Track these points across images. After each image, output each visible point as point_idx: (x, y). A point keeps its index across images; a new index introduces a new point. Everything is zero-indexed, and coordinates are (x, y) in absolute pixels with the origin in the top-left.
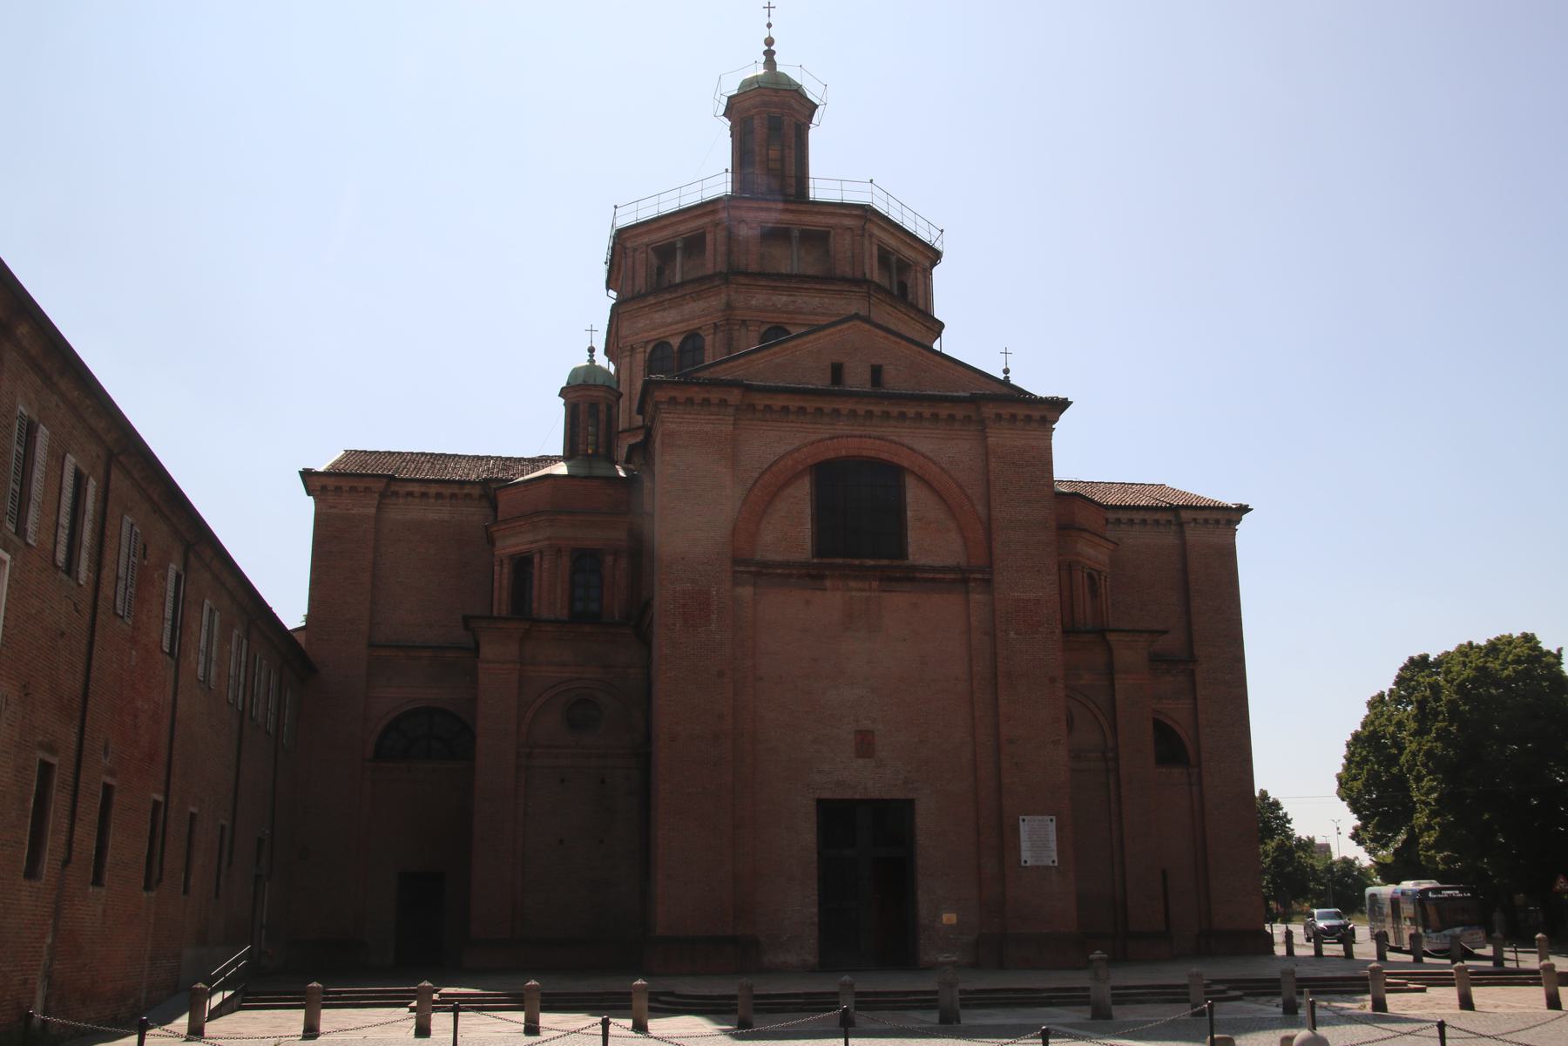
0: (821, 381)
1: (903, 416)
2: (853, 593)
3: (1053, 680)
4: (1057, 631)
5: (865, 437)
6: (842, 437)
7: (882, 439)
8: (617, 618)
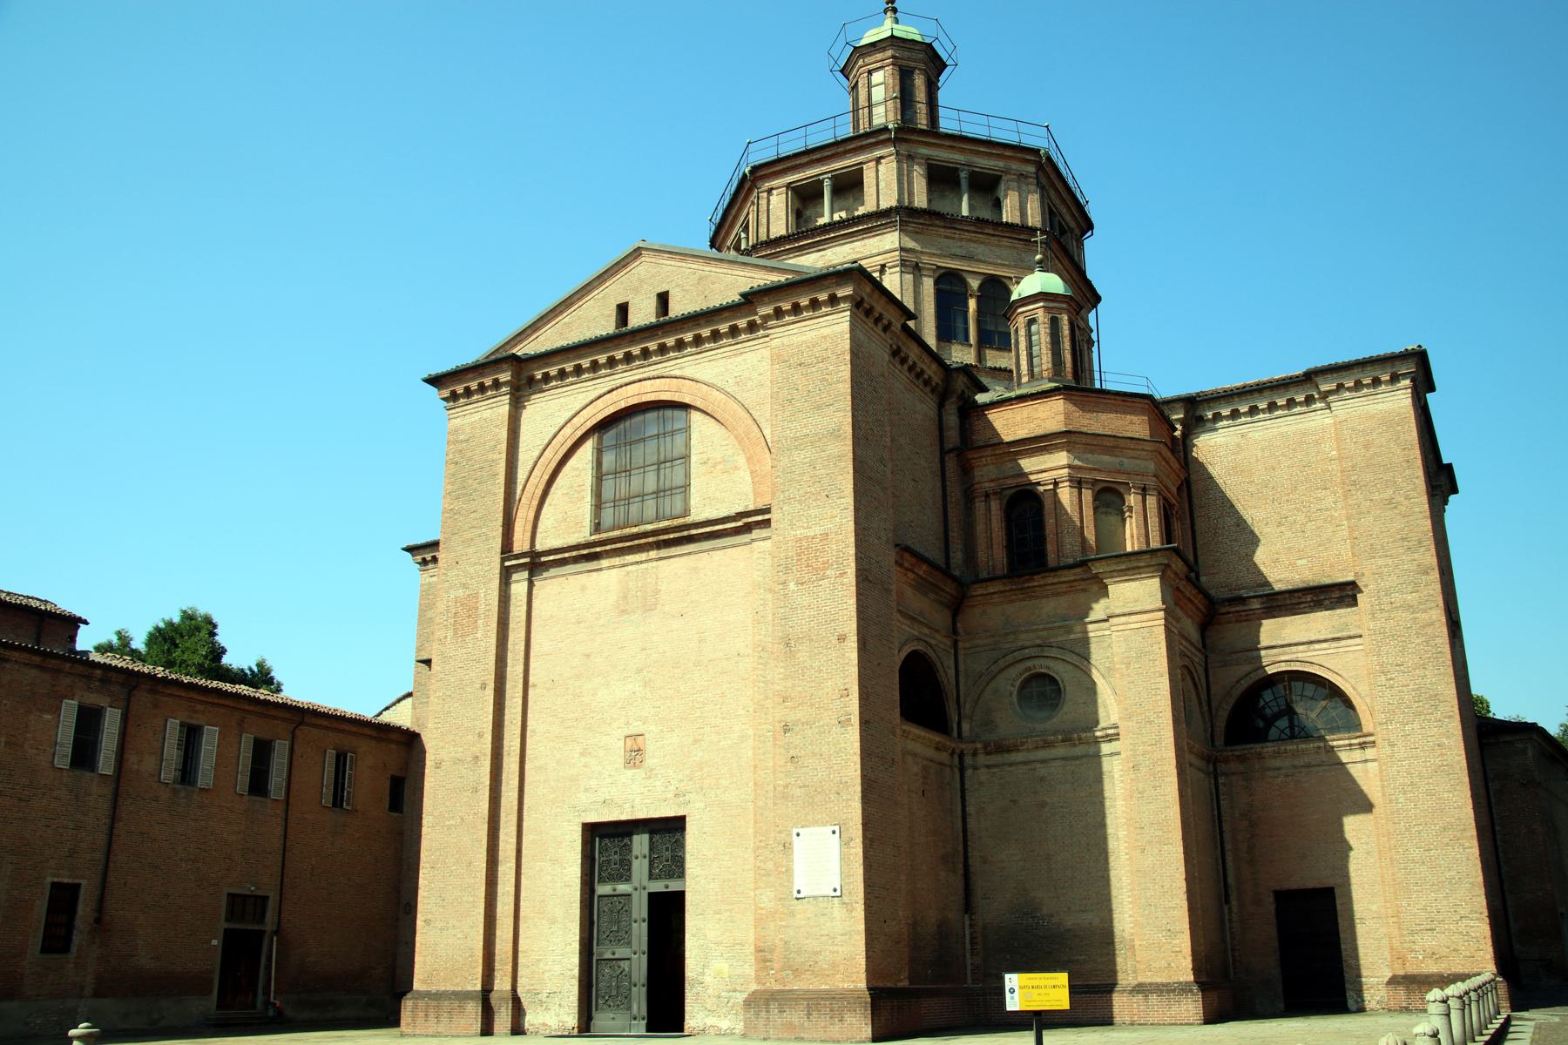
0: (608, 327)
1: (680, 345)
2: (630, 568)
3: (842, 639)
4: (849, 571)
6: (621, 386)
7: (663, 377)
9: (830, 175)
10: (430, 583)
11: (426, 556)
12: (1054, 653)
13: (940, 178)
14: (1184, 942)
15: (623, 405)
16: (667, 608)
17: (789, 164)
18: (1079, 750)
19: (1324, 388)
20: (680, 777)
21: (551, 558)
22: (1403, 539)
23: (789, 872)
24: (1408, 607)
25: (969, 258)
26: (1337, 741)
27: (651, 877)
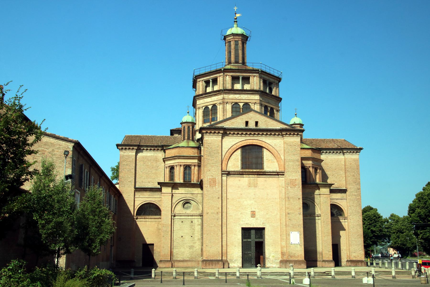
0: (243, 126)
2: (251, 178)
3: (299, 199)
5: (254, 139)
8: (195, 182)
9: (242, 76)
10: (123, 155)
11: (123, 147)
12: (308, 199)
13: (265, 82)
14: (331, 253)
15: (248, 144)
16: (259, 187)
17: (233, 71)
18: (312, 218)
19: (344, 151)
20: (264, 220)
21: (233, 173)
22: (355, 183)
23: (289, 239)
24: (355, 195)
25: (268, 103)
26: (340, 218)
27: (256, 238)
